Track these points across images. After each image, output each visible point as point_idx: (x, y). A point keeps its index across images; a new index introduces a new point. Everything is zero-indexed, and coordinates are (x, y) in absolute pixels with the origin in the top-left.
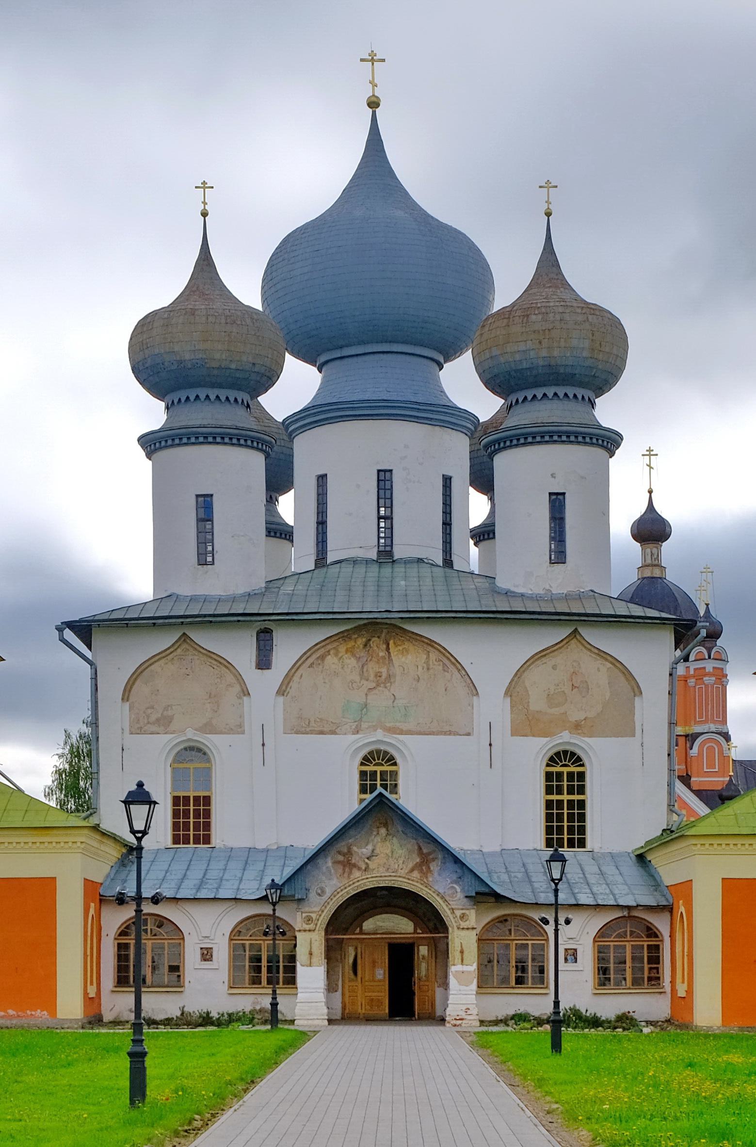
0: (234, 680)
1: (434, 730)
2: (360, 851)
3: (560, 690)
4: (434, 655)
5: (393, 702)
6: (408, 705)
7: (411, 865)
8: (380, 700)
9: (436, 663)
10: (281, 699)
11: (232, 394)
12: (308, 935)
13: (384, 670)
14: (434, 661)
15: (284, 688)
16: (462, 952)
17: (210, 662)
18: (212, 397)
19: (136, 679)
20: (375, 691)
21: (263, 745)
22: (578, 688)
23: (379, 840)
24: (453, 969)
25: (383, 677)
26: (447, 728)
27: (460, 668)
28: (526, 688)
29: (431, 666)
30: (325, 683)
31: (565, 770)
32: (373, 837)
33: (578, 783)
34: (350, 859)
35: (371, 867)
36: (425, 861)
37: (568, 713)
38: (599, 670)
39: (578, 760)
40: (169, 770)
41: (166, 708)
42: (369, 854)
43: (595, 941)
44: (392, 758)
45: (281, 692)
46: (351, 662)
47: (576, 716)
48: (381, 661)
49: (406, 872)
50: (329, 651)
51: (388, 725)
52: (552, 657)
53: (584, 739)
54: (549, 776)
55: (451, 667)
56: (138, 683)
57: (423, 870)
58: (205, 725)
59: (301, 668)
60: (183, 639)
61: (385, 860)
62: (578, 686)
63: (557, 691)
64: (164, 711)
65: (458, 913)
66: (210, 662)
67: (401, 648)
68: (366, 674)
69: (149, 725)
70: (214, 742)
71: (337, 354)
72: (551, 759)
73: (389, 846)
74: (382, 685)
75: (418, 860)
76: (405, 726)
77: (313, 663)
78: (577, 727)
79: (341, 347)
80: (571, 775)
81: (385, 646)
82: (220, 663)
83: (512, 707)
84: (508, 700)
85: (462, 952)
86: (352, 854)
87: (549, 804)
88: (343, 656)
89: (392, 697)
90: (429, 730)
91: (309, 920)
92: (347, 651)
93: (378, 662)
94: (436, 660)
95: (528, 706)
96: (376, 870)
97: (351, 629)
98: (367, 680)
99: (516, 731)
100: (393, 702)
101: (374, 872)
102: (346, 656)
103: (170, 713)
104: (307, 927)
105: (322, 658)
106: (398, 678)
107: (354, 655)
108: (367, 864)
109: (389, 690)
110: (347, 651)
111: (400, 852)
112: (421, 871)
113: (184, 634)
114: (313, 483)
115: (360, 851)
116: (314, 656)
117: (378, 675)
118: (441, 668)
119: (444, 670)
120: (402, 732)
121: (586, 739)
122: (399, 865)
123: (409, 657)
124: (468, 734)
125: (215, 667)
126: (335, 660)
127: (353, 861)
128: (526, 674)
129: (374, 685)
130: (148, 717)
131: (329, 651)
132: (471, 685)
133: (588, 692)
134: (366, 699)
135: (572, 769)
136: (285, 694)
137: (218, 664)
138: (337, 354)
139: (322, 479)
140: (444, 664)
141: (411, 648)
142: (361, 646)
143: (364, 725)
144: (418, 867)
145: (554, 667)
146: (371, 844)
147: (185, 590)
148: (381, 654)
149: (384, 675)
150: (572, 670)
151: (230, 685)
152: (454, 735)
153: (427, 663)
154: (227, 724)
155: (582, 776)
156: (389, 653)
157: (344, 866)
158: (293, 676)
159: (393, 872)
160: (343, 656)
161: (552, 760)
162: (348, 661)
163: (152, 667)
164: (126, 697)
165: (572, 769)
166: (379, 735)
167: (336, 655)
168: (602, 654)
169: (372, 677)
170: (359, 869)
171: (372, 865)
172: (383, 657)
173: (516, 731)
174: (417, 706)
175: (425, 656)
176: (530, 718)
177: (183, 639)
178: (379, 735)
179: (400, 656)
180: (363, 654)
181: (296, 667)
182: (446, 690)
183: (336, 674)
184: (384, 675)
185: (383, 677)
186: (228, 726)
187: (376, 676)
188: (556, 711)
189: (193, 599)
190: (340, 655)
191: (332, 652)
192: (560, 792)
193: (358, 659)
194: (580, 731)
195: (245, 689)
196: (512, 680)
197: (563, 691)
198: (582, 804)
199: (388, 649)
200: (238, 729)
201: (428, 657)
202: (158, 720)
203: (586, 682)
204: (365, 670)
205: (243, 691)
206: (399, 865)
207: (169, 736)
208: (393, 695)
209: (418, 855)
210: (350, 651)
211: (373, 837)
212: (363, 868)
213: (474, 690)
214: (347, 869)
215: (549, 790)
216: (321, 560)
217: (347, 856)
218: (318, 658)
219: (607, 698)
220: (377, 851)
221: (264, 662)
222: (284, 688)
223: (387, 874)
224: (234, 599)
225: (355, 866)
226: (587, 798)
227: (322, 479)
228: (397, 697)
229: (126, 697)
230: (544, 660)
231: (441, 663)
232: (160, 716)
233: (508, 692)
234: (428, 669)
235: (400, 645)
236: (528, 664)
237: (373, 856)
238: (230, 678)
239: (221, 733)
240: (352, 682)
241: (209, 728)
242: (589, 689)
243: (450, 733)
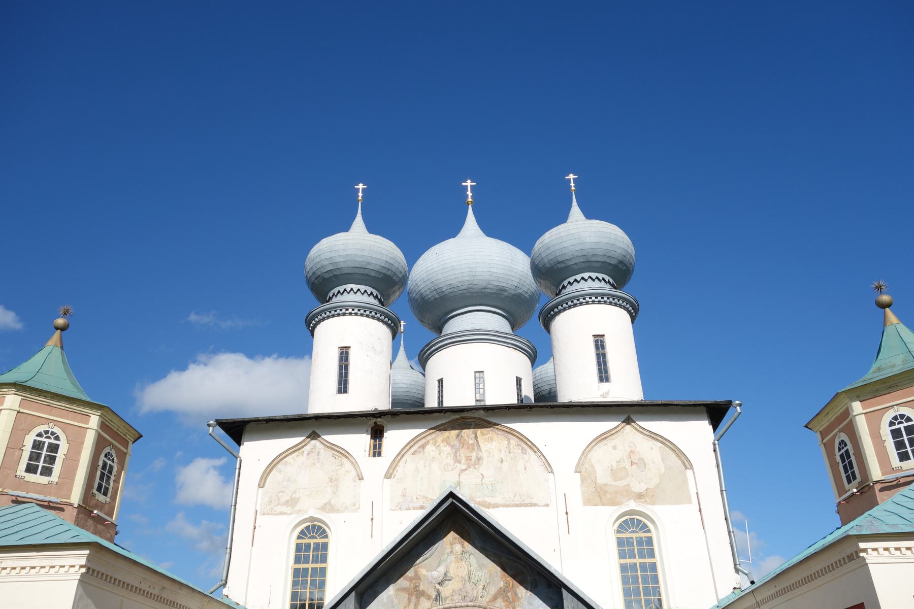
0: (352, 467)
1: (517, 503)
2: (429, 574)
3: (621, 466)
4: (514, 441)
5: (482, 480)
6: (494, 482)
7: (493, 590)
9: (516, 447)
14: (514, 445)
15: (391, 471)
17: (333, 454)
19: (272, 469)
20: (466, 472)
21: (372, 519)
22: (636, 464)
23: (453, 559)
25: (473, 460)
26: (527, 501)
27: (536, 450)
28: (592, 464)
29: (512, 450)
30: (425, 466)
32: (446, 556)
33: (647, 546)
34: (418, 584)
35: (443, 594)
36: (511, 584)
37: (630, 486)
38: (652, 449)
39: (645, 528)
41: (295, 492)
42: (441, 579)
45: (388, 475)
46: (448, 449)
48: (471, 447)
49: (487, 600)
50: (428, 441)
51: (478, 500)
52: (611, 439)
53: (647, 506)
54: (620, 542)
55: (529, 450)
56: (274, 471)
57: (509, 598)
58: (325, 505)
59: (405, 456)
60: (313, 436)
61: (460, 585)
62: (636, 462)
63: (619, 467)
64: (292, 494)
66: (333, 454)
67: (486, 437)
68: (458, 458)
69: (279, 506)
70: (333, 521)
72: (620, 526)
73: (466, 567)
74: (472, 467)
75: (502, 584)
76: (492, 501)
77: (416, 451)
78: (640, 496)
80: (640, 542)
81: (473, 436)
82: (341, 453)
83: (583, 480)
86: (420, 580)
87: (623, 568)
88: (439, 445)
89: (481, 476)
90: (513, 503)
92: (443, 441)
93: (468, 448)
94: (516, 445)
95: (596, 479)
96: (450, 599)
97: (446, 423)
98: (460, 462)
99: (588, 502)
100: (482, 480)
101: (447, 602)
102: (443, 444)
103: (297, 496)
105: (423, 447)
107: (449, 444)
108: (438, 591)
109: (478, 470)
110: (443, 441)
111: (479, 574)
113: (314, 432)
115: (429, 574)
116: (417, 446)
117: (469, 459)
118: (520, 451)
119: (523, 453)
121: (649, 506)
122: (477, 592)
123: (494, 443)
124: (547, 505)
125: (337, 457)
126: (434, 448)
127: (422, 588)
128: (591, 453)
129: (464, 467)
130: (279, 499)
131: (428, 441)
132: (546, 463)
133: (645, 467)
134: (459, 478)
135: (641, 535)
136: (392, 477)
137: (340, 455)
139: (441, 381)
140: (523, 449)
141: (495, 437)
142: (455, 436)
144: (502, 593)
145: (614, 448)
146: (443, 565)
148: (471, 442)
149: (474, 459)
150: (630, 451)
152: (535, 506)
153: (508, 447)
154: (344, 504)
156: (477, 441)
157: (410, 594)
158: (399, 462)
159: (471, 601)
160: (439, 445)
161: (622, 528)
162: (444, 449)
163: (286, 459)
164: (261, 485)
165: (641, 535)
167: (435, 445)
168: (654, 436)
169: (463, 461)
170: (429, 598)
171: (446, 591)
172: (473, 445)
173: (588, 502)
174: (502, 482)
175: (506, 442)
176: (599, 490)
177: (313, 436)
179: (486, 443)
180: (456, 443)
181: (401, 455)
182: (525, 469)
184: (474, 459)
185: (473, 460)
186: (344, 505)
187: (467, 459)
188: (621, 484)
190: (438, 444)
191: (431, 442)
193: (452, 447)
194: (643, 500)
195: (360, 474)
196: (581, 458)
197: (624, 467)
198: (653, 567)
199: (476, 437)
200: (355, 507)
201: (509, 443)
202: (287, 503)
203: (642, 458)
204: (458, 455)
205: (358, 476)
206: (477, 592)
207: (294, 515)
208: (482, 474)
209: (502, 578)
210: (446, 441)
211: (446, 556)
212: (434, 597)
214: (413, 599)
215: (622, 555)
217: (414, 582)
218: (420, 447)
219: (663, 472)
220: (451, 573)
221: (376, 452)
222: (391, 471)
223: (463, 604)
225: (423, 594)
226: (657, 560)
227: (441, 381)
228: (484, 476)
229: (262, 484)
230: (605, 442)
231: (520, 447)
232: (289, 498)
234: (510, 452)
235: (486, 435)
236: (592, 445)
237: (446, 580)
238: (347, 465)
239: (338, 511)
240: (447, 464)
241: (328, 507)
242: (646, 465)
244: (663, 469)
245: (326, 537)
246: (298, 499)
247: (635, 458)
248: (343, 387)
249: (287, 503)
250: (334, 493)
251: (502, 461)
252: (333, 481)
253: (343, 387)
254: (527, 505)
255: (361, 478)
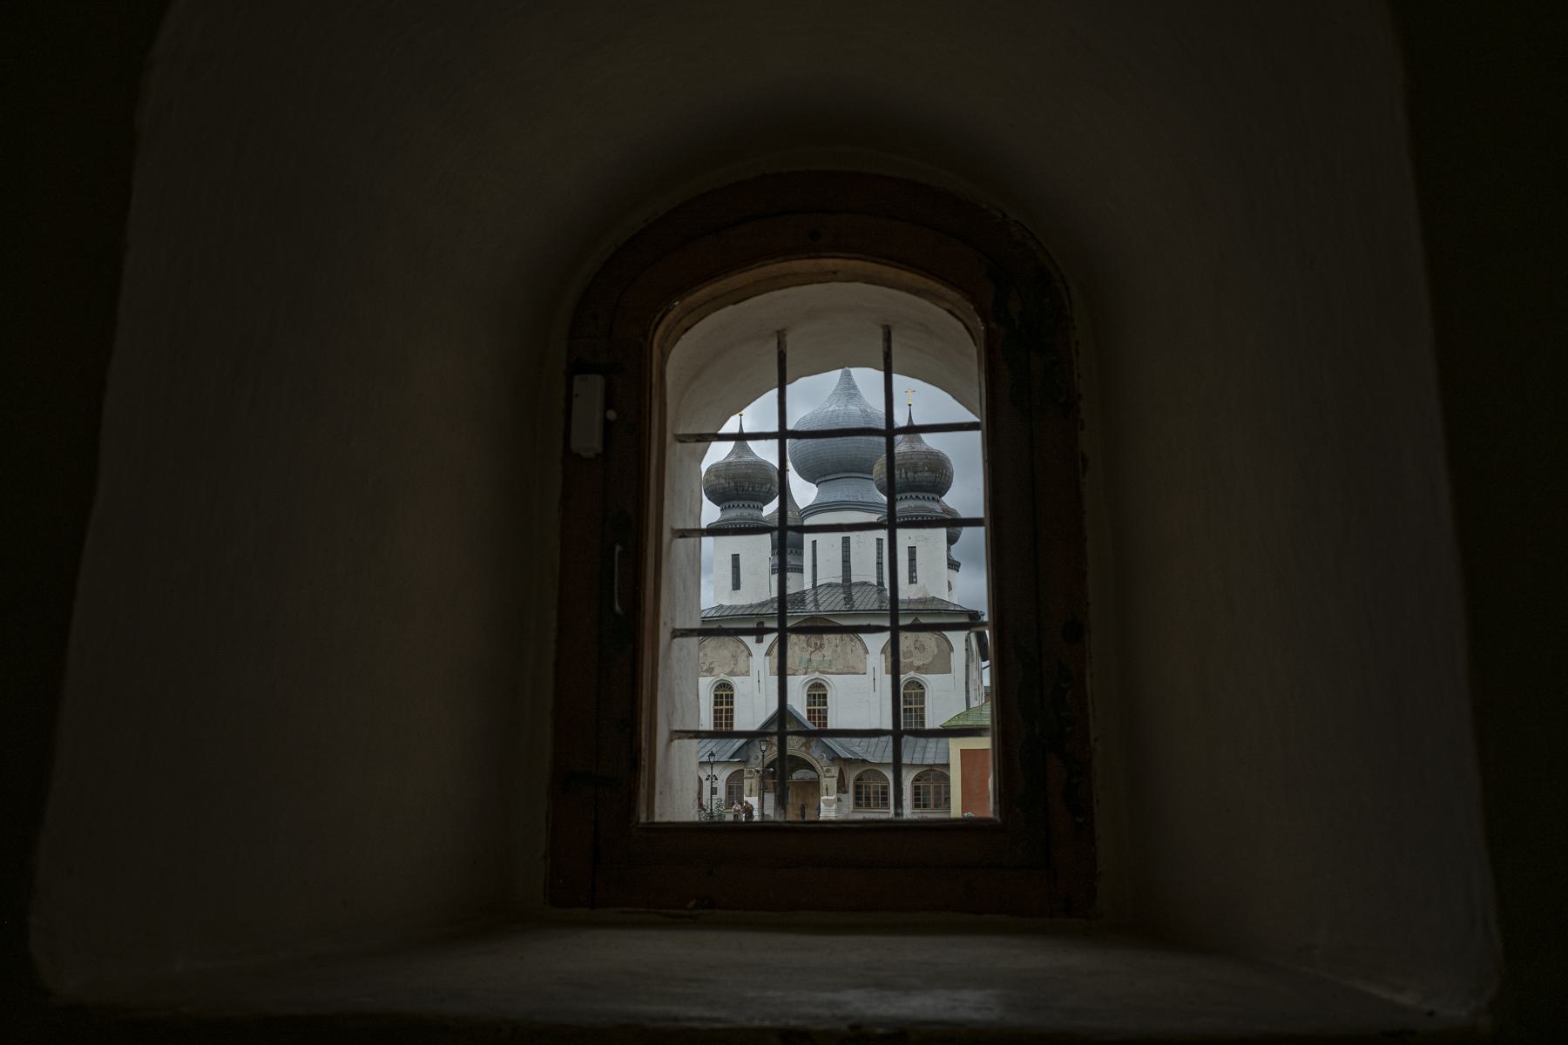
8: (817, 657)
10: (768, 658)
11: (751, 504)
12: (749, 781)
13: (818, 642)
16: (827, 789)
18: (746, 506)
24: (822, 798)
31: (913, 691)
39: (920, 686)
40: (713, 695)
41: (710, 664)
43: (912, 783)
44: (823, 686)
47: (918, 663)
65: (825, 769)
70: (735, 681)
71: (823, 479)
76: (830, 671)
78: (918, 669)
79: (825, 475)
80: (916, 694)
84: (883, 656)
85: (827, 789)
91: (750, 772)
104: (749, 776)
106: (826, 646)
112: (806, 747)
114: (811, 545)
117: (816, 644)
120: (828, 673)
124: (865, 674)
138: (823, 479)
143: (810, 670)
147: (726, 603)
151: (743, 651)
155: (923, 695)
166: (817, 675)
178: (817, 675)
183: (795, 644)
189: (730, 607)
192: (911, 704)
200: (747, 673)
202: (707, 671)
203: (923, 645)
213: (867, 652)
216: (814, 586)
224: (751, 606)
233: (882, 652)
238: (743, 648)
241: (732, 673)
243: (854, 673)
244: (936, 652)
245: (732, 690)
246: (713, 669)
247: (918, 645)
248: (736, 585)
249: (707, 671)
250: (735, 665)
251: (837, 646)
252: (734, 657)
253: (736, 585)
254: (852, 673)
255: (750, 654)
